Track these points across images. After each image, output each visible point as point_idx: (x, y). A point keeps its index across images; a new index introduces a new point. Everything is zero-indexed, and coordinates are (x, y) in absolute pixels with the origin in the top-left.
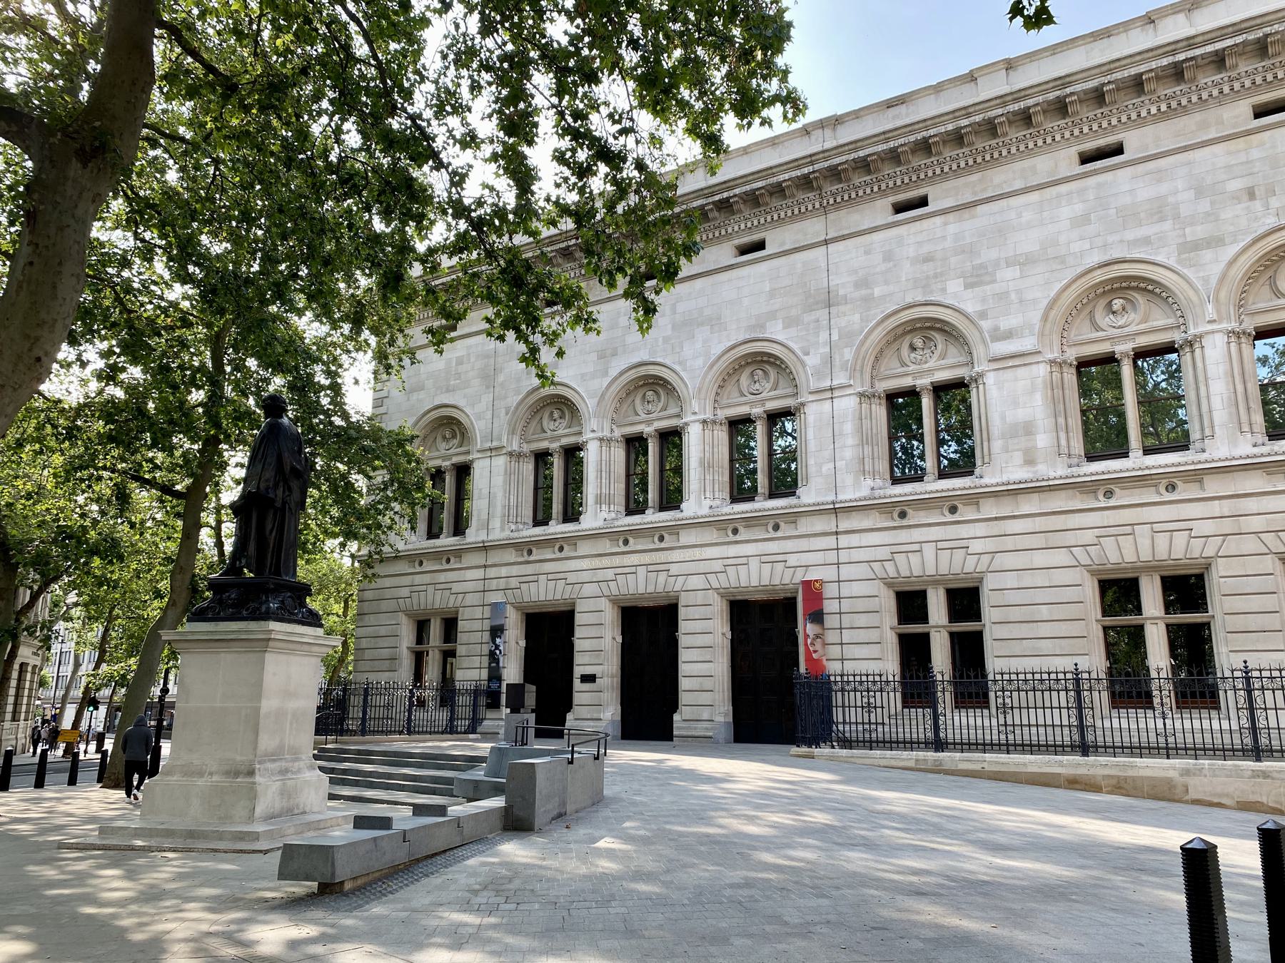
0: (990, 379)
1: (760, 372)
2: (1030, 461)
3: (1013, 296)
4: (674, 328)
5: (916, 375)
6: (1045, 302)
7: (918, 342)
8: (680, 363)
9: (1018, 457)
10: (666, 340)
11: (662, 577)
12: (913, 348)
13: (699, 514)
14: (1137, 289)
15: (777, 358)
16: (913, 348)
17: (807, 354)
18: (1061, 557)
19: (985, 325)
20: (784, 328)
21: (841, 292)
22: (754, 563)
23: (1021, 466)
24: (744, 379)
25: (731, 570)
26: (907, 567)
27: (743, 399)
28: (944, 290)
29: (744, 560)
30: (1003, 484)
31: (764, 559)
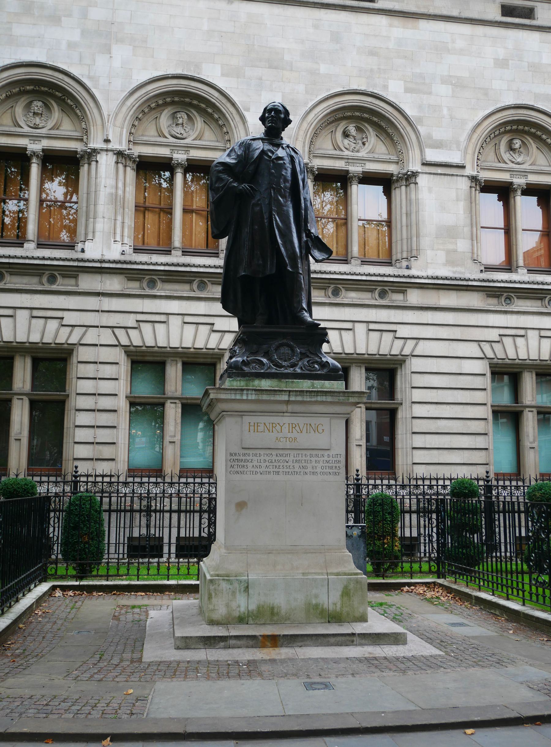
0: (422, 180)
1: (186, 117)
2: (450, 262)
3: (445, 111)
4: (84, 33)
5: (347, 159)
6: (470, 125)
7: (352, 129)
8: (90, 77)
9: (441, 256)
10: (71, 45)
11: (53, 325)
12: (346, 135)
13: (107, 257)
14: (535, 137)
15: (213, 106)
16: (346, 135)
17: (248, 110)
18: (473, 350)
19: (421, 129)
20: (223, 75)
21: (287, 57)
22: (175, 322)
23: (445, 265)
24: (164, 119)
25: (147, 328)
26: (339, 343)
27: (162, 139)
28: (386, 87)
29: (163, 318)
30: (432, 278)
31: (188, 319)
